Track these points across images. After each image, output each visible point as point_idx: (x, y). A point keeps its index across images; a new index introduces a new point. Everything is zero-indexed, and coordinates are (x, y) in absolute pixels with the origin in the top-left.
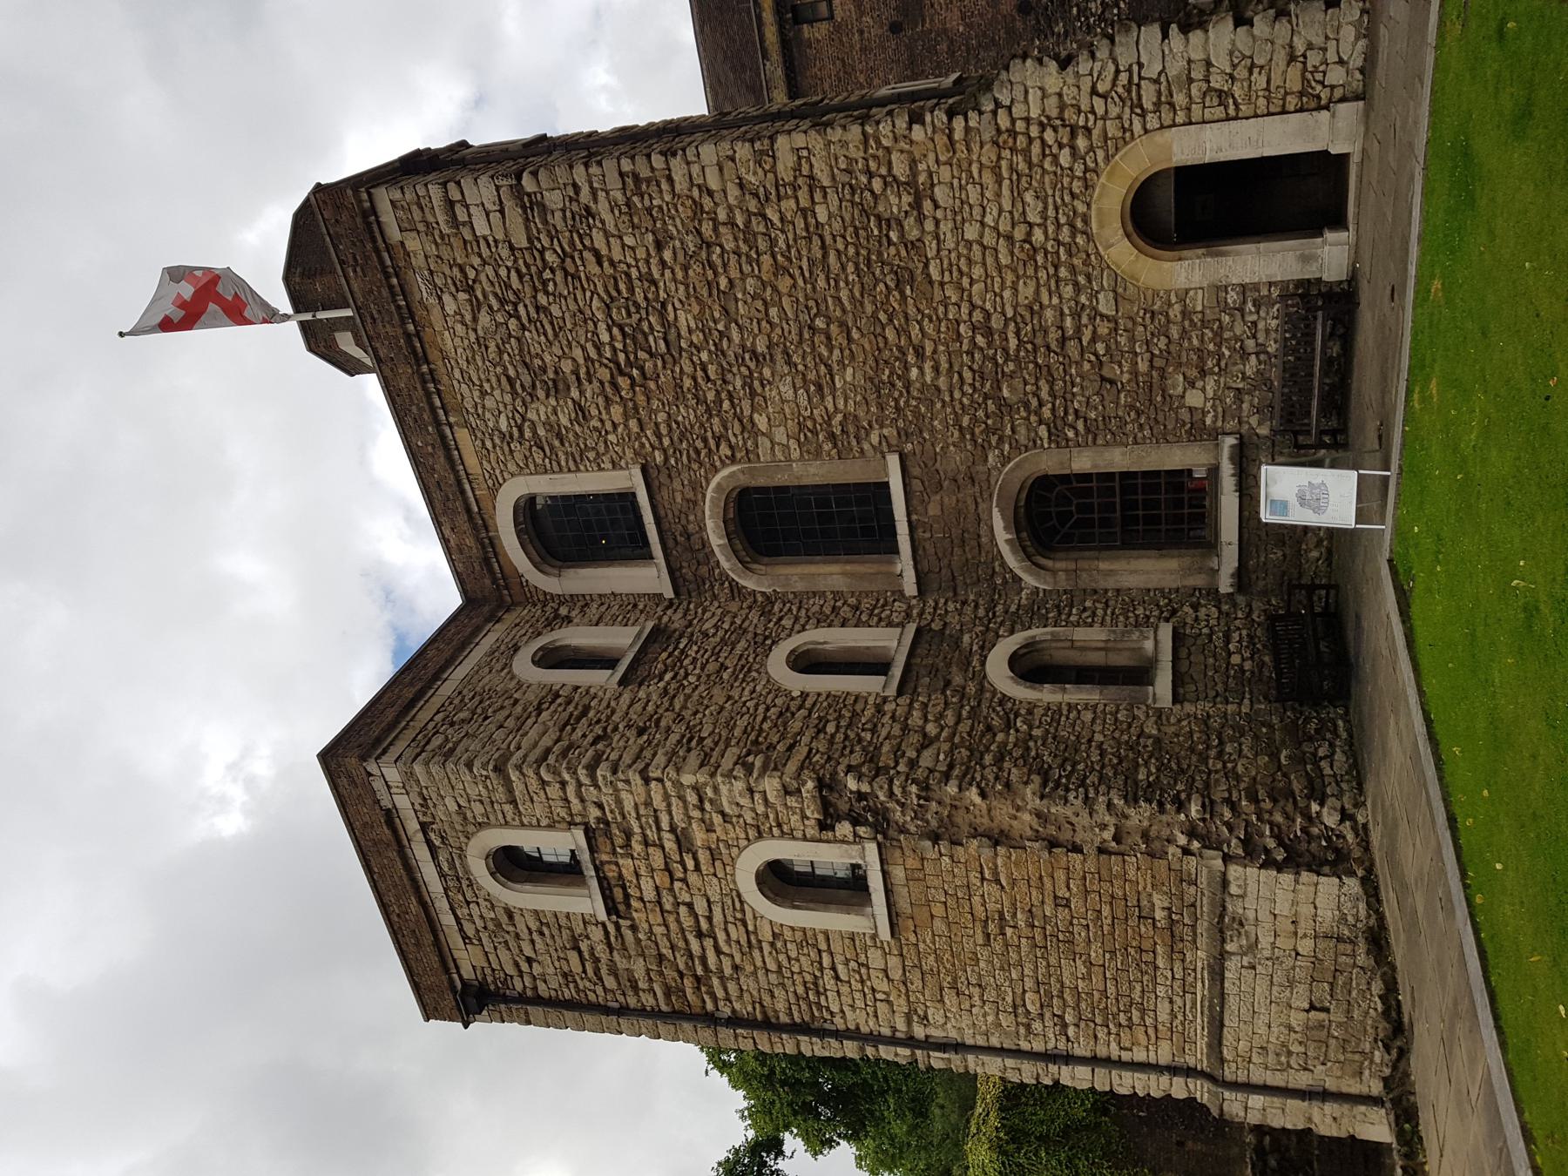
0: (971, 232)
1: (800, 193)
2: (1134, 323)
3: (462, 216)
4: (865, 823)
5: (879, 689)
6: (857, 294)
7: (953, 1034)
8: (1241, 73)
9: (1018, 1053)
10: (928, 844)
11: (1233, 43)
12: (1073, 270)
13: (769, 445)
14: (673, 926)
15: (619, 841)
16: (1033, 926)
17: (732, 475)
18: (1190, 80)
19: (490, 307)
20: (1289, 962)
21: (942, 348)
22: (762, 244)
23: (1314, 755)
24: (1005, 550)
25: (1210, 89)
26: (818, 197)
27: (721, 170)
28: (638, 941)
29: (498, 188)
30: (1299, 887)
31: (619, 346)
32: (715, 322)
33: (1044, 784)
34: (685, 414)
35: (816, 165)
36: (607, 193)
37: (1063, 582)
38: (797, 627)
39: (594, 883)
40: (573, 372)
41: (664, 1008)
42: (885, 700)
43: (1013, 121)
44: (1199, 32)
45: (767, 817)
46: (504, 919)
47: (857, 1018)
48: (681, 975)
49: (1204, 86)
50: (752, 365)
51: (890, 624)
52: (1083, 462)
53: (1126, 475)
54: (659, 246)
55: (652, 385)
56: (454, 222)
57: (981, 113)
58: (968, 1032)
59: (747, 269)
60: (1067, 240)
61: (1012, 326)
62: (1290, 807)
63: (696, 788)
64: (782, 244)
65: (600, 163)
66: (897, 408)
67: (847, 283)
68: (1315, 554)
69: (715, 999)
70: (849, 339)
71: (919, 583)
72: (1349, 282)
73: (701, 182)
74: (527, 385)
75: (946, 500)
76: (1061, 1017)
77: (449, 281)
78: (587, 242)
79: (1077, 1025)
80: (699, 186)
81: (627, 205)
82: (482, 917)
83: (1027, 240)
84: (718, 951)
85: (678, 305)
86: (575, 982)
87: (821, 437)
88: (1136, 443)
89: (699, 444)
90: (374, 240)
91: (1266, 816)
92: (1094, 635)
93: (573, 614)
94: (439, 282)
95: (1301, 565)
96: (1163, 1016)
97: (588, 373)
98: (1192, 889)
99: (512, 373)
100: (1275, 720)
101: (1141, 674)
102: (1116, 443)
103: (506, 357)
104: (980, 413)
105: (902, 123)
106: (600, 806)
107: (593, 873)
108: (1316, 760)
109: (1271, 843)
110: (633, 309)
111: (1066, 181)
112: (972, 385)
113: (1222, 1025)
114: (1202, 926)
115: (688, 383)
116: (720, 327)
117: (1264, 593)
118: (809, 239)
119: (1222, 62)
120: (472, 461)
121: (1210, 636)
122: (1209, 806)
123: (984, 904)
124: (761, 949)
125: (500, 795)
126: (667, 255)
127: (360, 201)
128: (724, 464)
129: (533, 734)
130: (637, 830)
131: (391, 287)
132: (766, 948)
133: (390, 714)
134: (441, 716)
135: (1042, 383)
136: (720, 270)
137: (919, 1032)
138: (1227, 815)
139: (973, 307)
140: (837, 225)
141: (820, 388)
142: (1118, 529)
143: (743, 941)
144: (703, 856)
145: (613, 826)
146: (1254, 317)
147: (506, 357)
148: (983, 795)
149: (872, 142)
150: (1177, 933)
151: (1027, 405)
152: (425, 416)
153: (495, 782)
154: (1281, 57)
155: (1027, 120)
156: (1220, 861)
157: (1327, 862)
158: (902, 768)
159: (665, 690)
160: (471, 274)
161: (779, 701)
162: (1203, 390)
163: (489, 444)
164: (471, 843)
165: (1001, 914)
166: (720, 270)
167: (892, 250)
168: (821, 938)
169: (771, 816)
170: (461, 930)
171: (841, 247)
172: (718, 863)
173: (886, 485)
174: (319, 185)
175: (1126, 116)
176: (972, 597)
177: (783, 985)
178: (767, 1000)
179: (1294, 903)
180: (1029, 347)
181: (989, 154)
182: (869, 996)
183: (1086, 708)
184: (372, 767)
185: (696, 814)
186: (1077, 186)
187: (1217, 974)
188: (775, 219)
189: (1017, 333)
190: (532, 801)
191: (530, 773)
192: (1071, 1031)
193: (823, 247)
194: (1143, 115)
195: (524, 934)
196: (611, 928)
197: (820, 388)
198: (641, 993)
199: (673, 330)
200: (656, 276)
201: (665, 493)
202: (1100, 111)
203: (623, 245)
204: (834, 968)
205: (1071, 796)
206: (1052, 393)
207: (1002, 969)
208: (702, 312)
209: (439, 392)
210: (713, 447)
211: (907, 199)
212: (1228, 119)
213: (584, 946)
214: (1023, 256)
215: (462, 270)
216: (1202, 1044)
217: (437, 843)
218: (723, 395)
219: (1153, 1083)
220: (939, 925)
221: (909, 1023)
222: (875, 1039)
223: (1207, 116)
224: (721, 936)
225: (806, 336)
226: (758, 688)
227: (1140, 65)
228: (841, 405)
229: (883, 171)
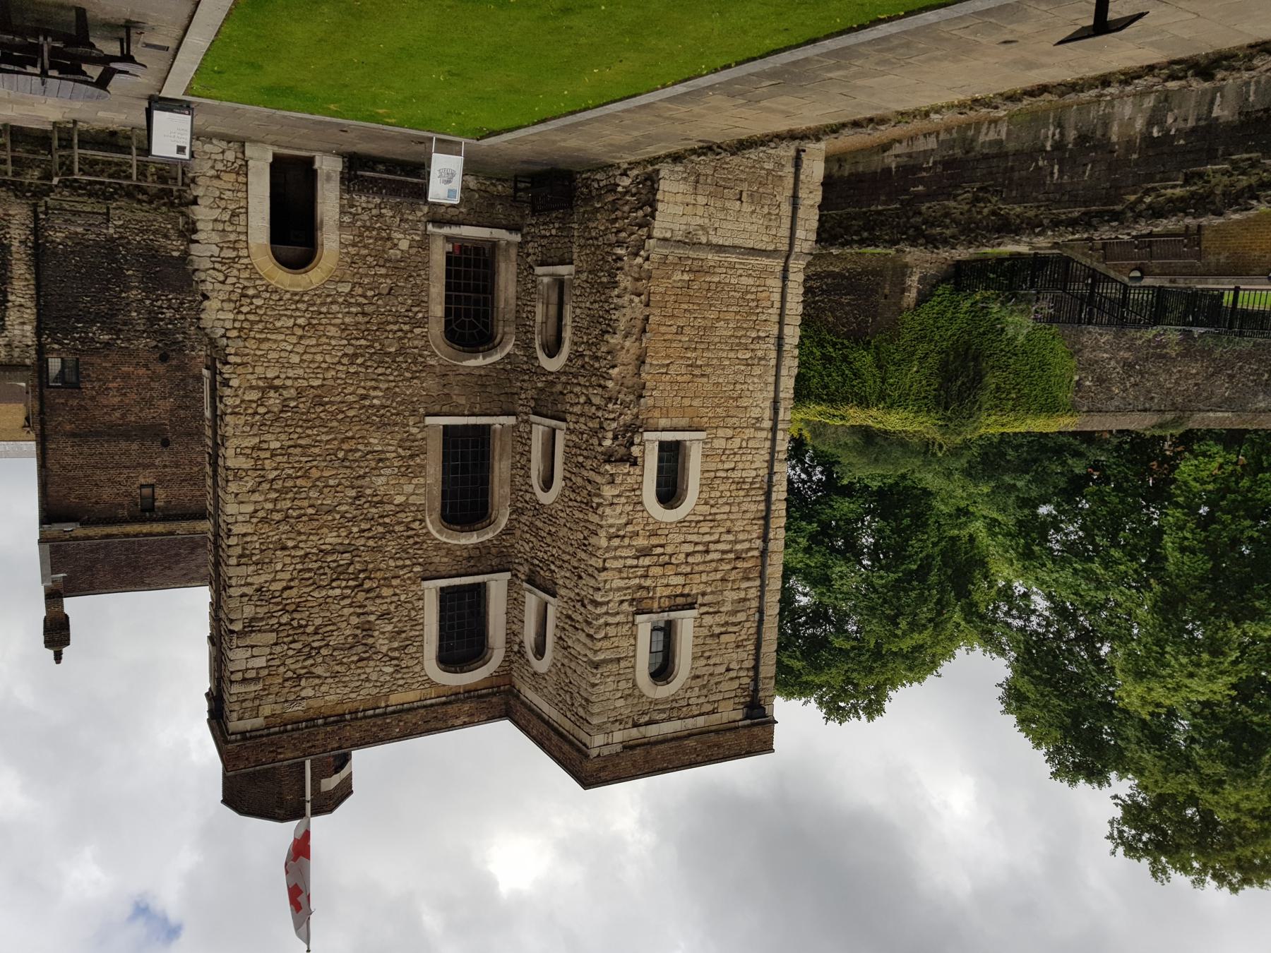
0: (295, 359)
1: (262, 457)
2: (358, 273)
3: (252, 674)
4: (632, 437)
5: (563, 433)
6: (325, 430)
7: (768, 404)
8: (223, 204)
9: (778, 366)
10: (642, 400)
11: (206, 207)
12: (323, 304)
13: (414, 497)
14: (701, 568)
15: (643, 594)
16: (695, 348)
17: (432, 523)
18: (224, 230)
19: (312, 665)
20: (711, 209)
21: (362, 384)
22: (290, 483)
23: (597, 189)
24: (489, 360)
25: (230, 221)
26: (264, 446)
27: (242, 502)
28: (712, 593)
30: (666, 200)
31: (344, 584)
32: (334, 520)
33: (608, 332)
34: (391, 547)
35: (246, 445)
36: (248, 576)
37: (511, 329)
38: (530, 490)
39: (673, 615)
40: (358, 617)
41: (758, 583)
42: (568, 429)
43: (234, 328)
44: (198, 224)
45: (629, 497)
46: (699, 682)
47: (761, 460)
48: (735, 568)
49: (227, 223)
50: (363, 500)
51: (531, 432)
52: (438, 310)
53: (448, 287)
54: (284, 548)
55: (371, 566)
56: (256, 680)
57: (227, 346)
58: (765, 394)
59: (303, 495)
60: (305, 305)
61: (353, 342)
62: (620, 202)
63: (610, 538)
64: (290, 472)
65: (230, 578)
66: (397, 414)
67: (318, 435)
68: (500, 188)
69: (750, 549)
70: (352, 438)
71: (508, 415)
72: (344, 157)
73: (248, 516)
74: (364, 649)
75: (456, 392)
76: (753, 339)
77: (293, 690)
78: (277, 594)
79: (758, 331)
80: (251, 517)
81: (257, 564)
82: (698, 697)
83: (303, 327)
84: (718, 542)
85: (322, 542)
86: (742, 641)
87: (412, 463)
88: (428, 279)
89: (411, 541)
90: (261, 736)
91: (626, 215)
92: (539, 310)
93: (518, 641)
94: (293, 697)
95: (507, 196)
96: (751, 281)
97: (359, 607)
98: (670, 258)
99: (355, 658)
100: (582, 210)
101: (560, 283)
102: (428, 291)
103: (345, 660)
104: (404, 365)
105: (228, 391)
106: (622, 602)
107: (666, 614)
108: (600, 188)
109: (640, 213)
110: (322, 571)
111: (271, 302)
112: (387, 368)
113: (753, 249)
114: (692, 254)
115: (371, 543)
116: (338, 516)
117: (522, 217)
118: (289, 455)
119: (216, 213)
120: (411, 696)
121: (542, 246)
122: (620, 244)
123: (683, 375)
124: (716, 514)
125: (614, 667)
126: (290, 544)
127: (236, 741)
128: (425, 527)
129: (579, 647)
130: (637, 581)
131: (293, 730)
132: (714, 510)
133: (566, 747)
134: (569, 716)
135: (388, 328)
136: (303, 512)
137: (767, 424)
138: (623, 234)
139: (339, 362)
140: (283, 437)
141: (381, 460)
142: (482, 296)
143: (712, 524)
144: (654, 541)
145: (635, 596)
146: (359, 209)
147: (345, 660)
148: (614, 367)
149: (237, 410)
150: (696, 269)
151: (401, 338)
152: (379, 723)
153: (605, 670)
154: (216, 183)
155: (234, 320)
156: (651, 241)
157: (652, 186)
158: (600, 414)
159: (561, 567)
160: (290, 674)
161: (567, 493)
162: (399, 239)
163: (401, 682)
164: (647, 694)
166: (303, 512)
167: (301, 406)
168: (706, 475)
169: (628, 494)
170: (708, 713)
171: (296, 436)
172: (659, 532)
173: (445, 427)
174: (223, 801)
175: (239, 266)
176: (519, 384)
177: (739, 504)
178: (748, 515)
179: (676, 203)
180: (366, 333)
181: (251, 344)
182: (744, 451)
183: (574, 312)
184: (594, 753)
185: (627, 541)
186: (276, 297)
187: (720, 248)
188: (276, 473)
189: (357, 339)
191: (599, 644)
192: (762, 334)
193: (295, 446)
194: (240, 257)
195: (711, 669)
197: (381, 460)
198: (748, 597)
199: (337, 547)
200: (302, 553)
201: (441, 568)
202: (234, 280)
203: (282, 571)
204: (727, 470)
205: (614, 317)
206: (396, 323)
207: (723, 369)
208: (327, 527)
209: (364, 710)
210: (413, 532)
211: (272, 394)
212: (247, 213)
213: (717, 630)
214: (312, 331)
215: (287, 680)
216: (766, 261)
217: (646, 718)
218: (381, 521)
219: (795, 291)
220: (696, 403)
221: (762, 429)
223: (244, 223)
224: (707, 538)
225: (348, 464)
226: (560, 508)
227: (212, 256)
228: (393, 448)
229: (254, 405)
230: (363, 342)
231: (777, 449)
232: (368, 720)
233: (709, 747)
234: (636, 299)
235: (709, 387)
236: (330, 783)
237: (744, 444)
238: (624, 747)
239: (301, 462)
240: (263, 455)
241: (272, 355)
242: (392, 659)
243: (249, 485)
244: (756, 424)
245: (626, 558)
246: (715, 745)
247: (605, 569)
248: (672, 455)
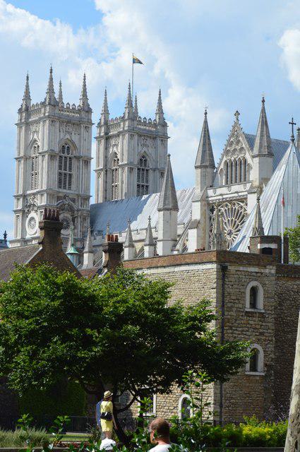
9: (221, 398)
39: (253, 310)
130: (263, 324)
220: (248, 384)
236: (273, 246)
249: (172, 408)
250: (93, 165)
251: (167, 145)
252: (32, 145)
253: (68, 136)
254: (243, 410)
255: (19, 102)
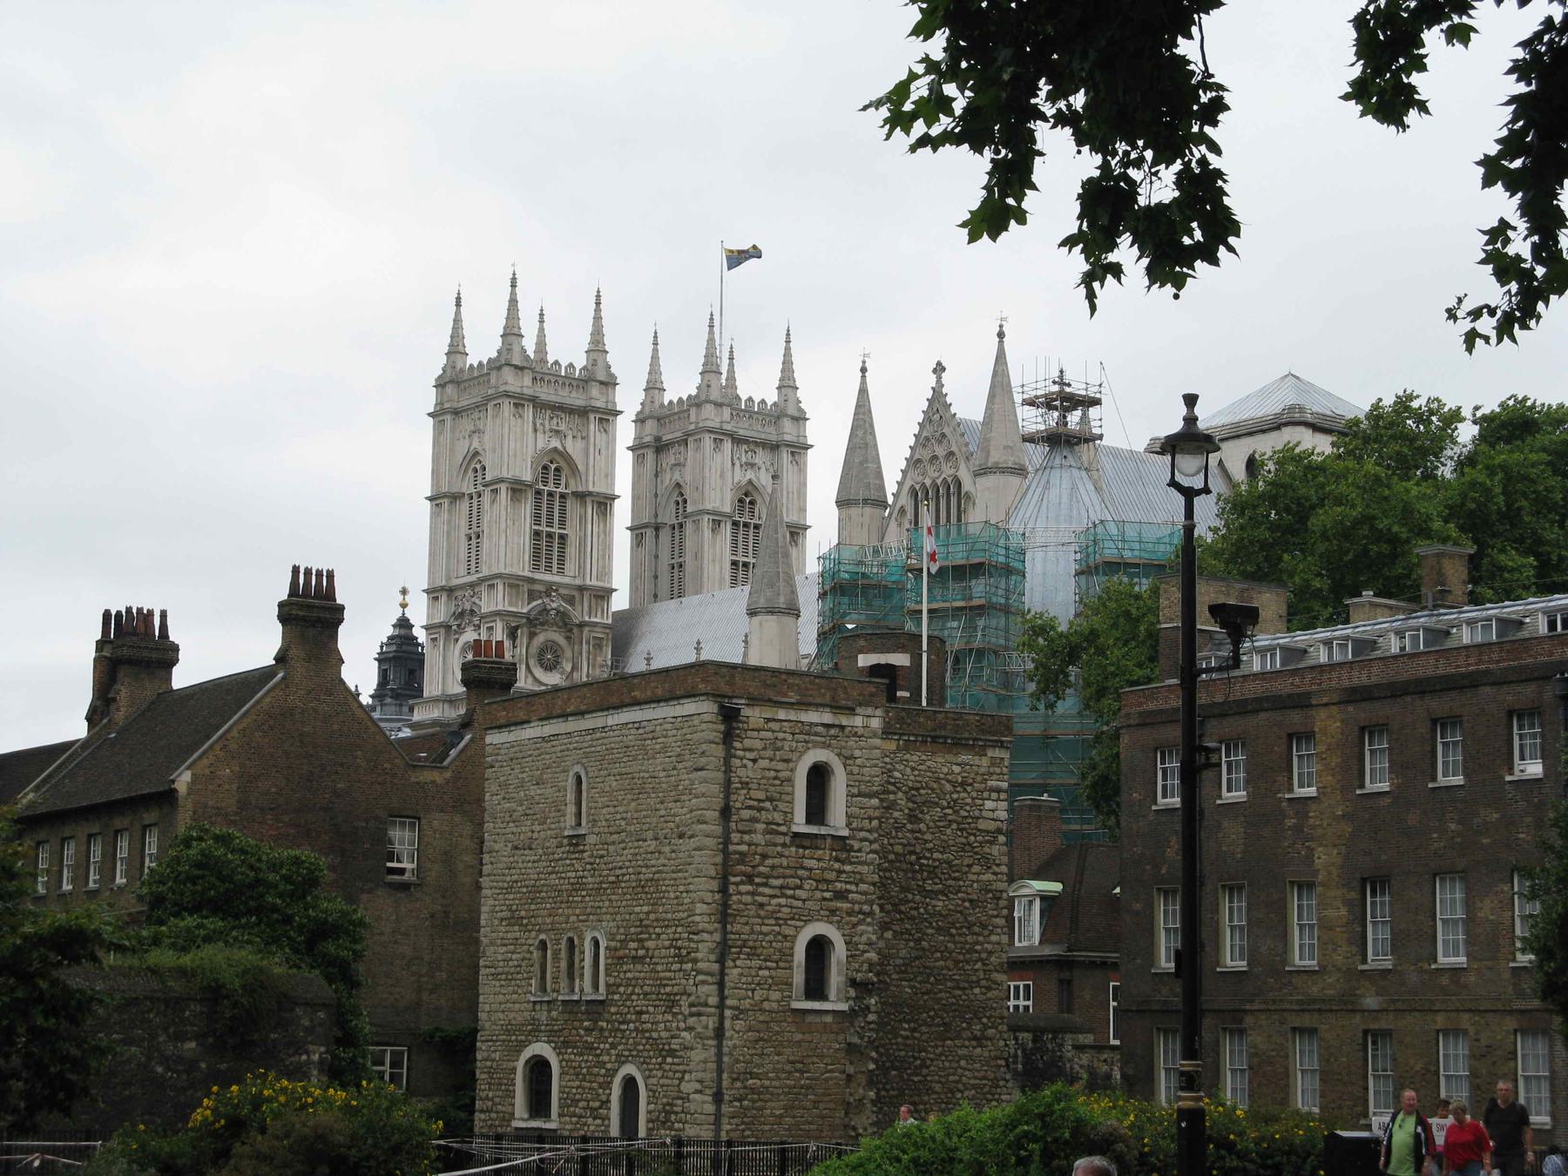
0: (963, 1063)
3: (994, 795)
7: (728, 1034)
22: (968, 956)
29: (1002, 821)
41: (732, 848)
45: (857, 950)
48: (753, 867)
54: (971, 901)
55: (910, 875)
56: (992, 790)
59: (958, 946)
63: (871, 914)
64: (967, 967)
70: (923, 994)
79: (741, 1107)
85: (946, 903)
86: (743, 788)
99: (922, 791)
104: (884, 1059)
106: (859, 850)
118: (967, 982)
124: (775, 925)
130: (848, 868)
131: (968, 739)
132: (777, 928)
135: (895, 1093)
137: (728, 1013)
140: (972, 997)
141: (901, 972)
143: (778, 915)
151: (887, 1083)
155: (1000, 1094)
160: (969, 789)
165: (806, 1072)
168: (787, 965)
170: (775, 720)
171: (964, 997)
172: (827, 913)
177: (752, 932)
178: (743, 920)
181: (991, 1075)
185: (857, 907)
188: (976, 967)
189: (920, 1081)
190: (861, 808)
191: (877, 814)
193: (964, 988)
196: (783, 829)
198: (739, 835)
200: (960, 895)
203: (973, 881)
206: (893, 1096)
207: (774, 1068)
208: (941, 915)
211: (979, 1033)
213: (767, 804)
217: (832, 732)
220: (799, 1037)
222: (721, 985)
225: (927, 971)
230: (916, 1079)
231: (715, 987)
232: (915, 732)
233: (775, 686)
234: (861, 1131)
235: (788, 1051)
236: (900, 659)
237: (750, 993)
238: (853, 709)
239: (961, 975)
240: (983, 983)
241: (977, 1066)
242: (894, 784)
243: (993, 959)
244: (740, 1012)
245: (857, 892)
246: (768, 686)
247: (874, 884)
248: (816, 988)
249: (597, 1104)
250: (622, 514)
251: (805, 464)
252: (469, 463)
253: (555, 443)
254: (786, 1108)
255: (436, 364)
